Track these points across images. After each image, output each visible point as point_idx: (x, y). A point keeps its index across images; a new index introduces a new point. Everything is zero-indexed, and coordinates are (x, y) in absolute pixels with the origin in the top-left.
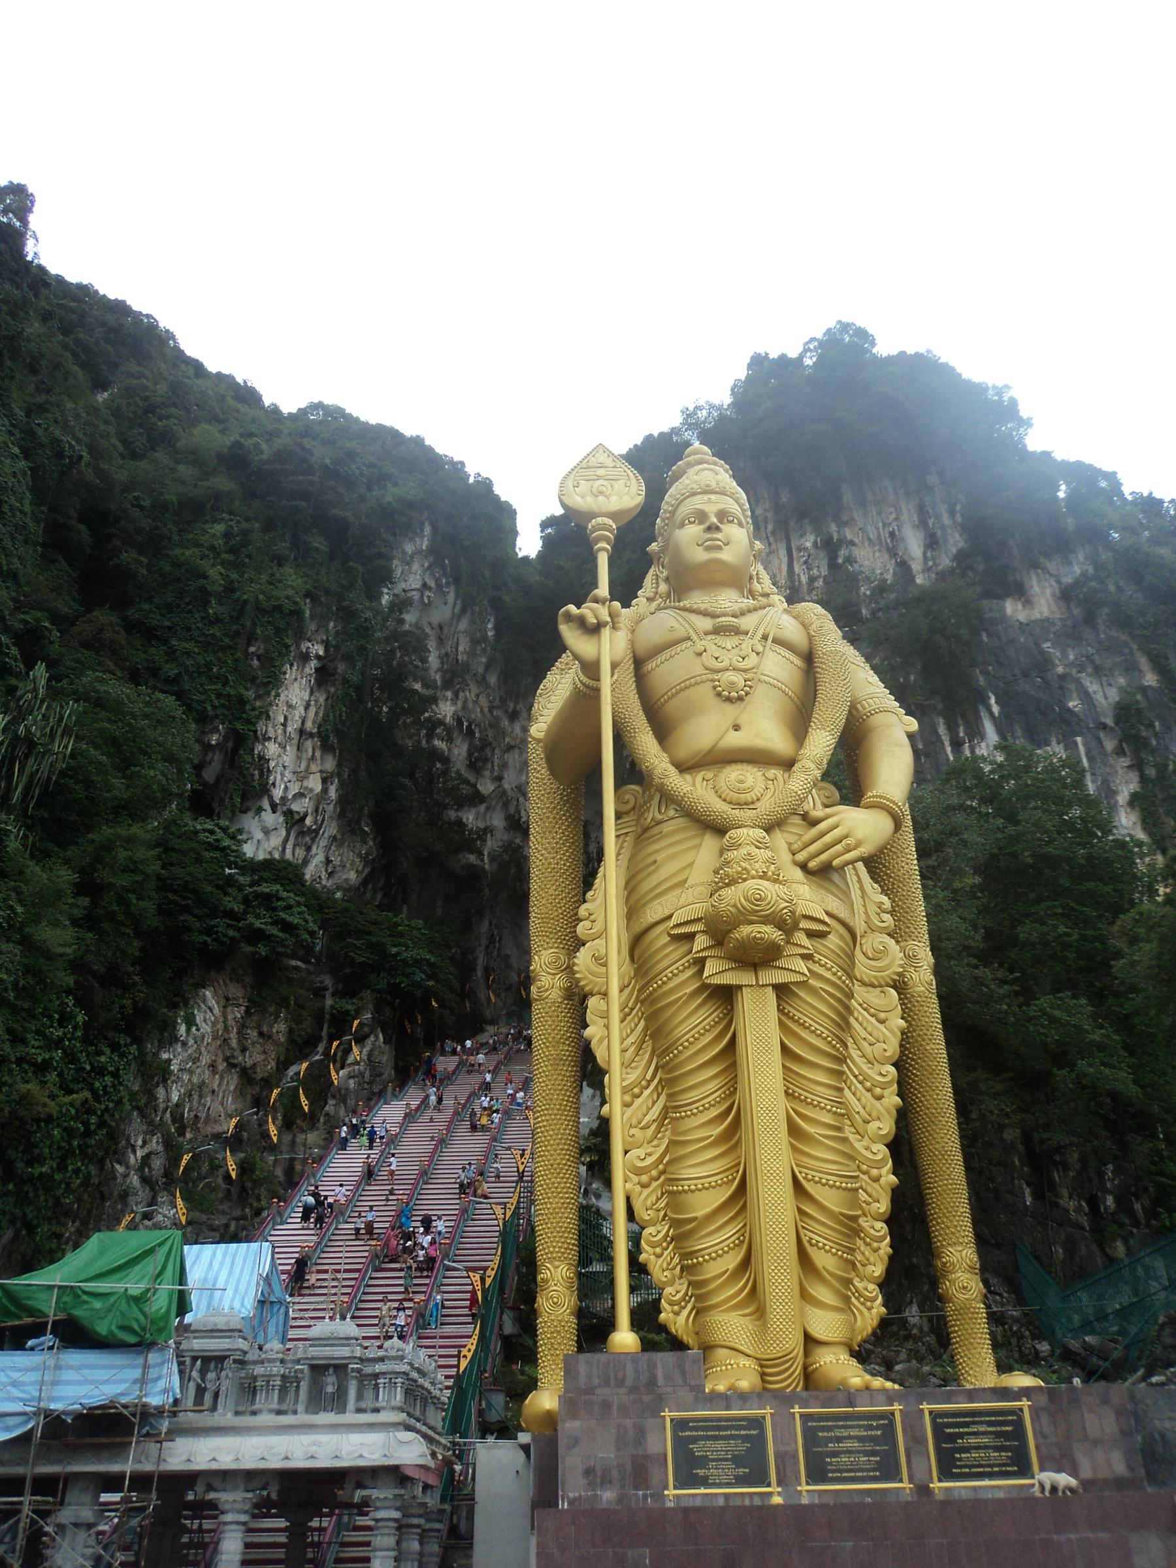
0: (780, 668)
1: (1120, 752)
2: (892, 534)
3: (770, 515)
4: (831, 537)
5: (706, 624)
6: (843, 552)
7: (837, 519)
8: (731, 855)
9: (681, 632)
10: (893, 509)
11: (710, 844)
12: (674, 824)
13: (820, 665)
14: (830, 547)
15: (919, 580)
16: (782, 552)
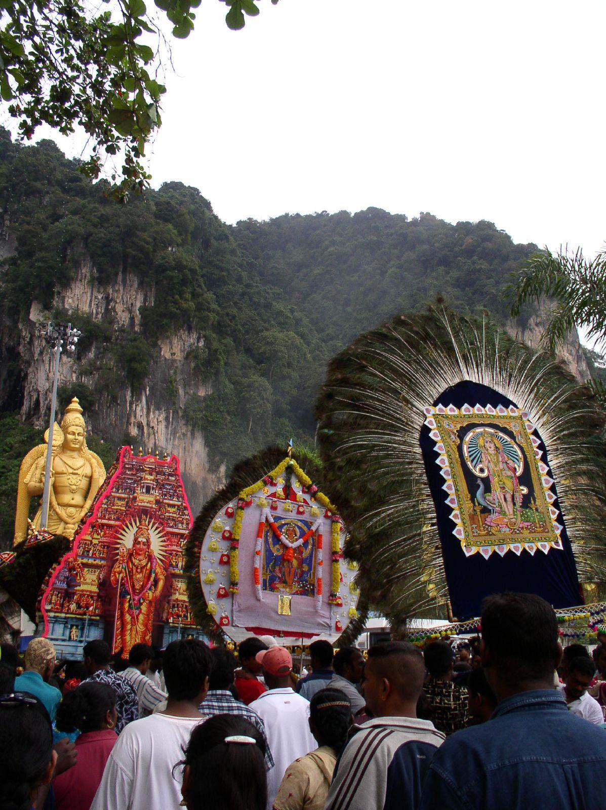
0: (83, 483)
1: (183, 417)
2: (132, 304)
3: (88, 275)
4: (109, 295)
5: (71, 471)
6: (112, 304)
7: (113, 287)
8: (68, 531)
9: (65, 471)
10: (134, 293)
11: (62, 524)
12: (55, 517)
13: (93, 482)
14: (108, 300)
15: (136, 329)
16: (89, 294)
